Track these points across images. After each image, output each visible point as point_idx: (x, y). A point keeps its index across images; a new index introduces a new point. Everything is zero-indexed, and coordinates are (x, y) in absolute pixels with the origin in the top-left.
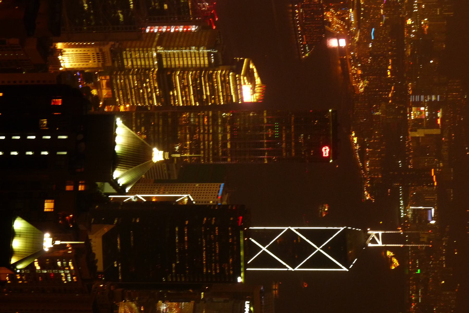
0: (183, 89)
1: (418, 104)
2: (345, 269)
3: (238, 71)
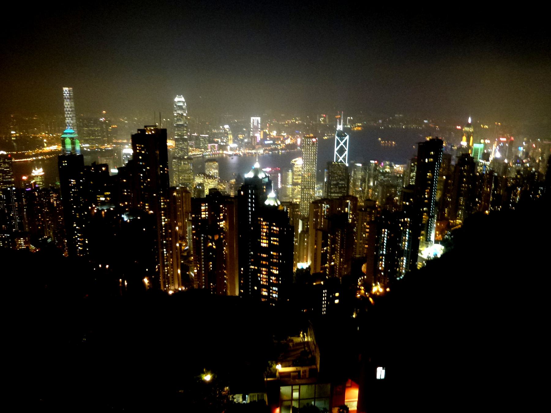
0: (298, 179)
3: (294, 164)
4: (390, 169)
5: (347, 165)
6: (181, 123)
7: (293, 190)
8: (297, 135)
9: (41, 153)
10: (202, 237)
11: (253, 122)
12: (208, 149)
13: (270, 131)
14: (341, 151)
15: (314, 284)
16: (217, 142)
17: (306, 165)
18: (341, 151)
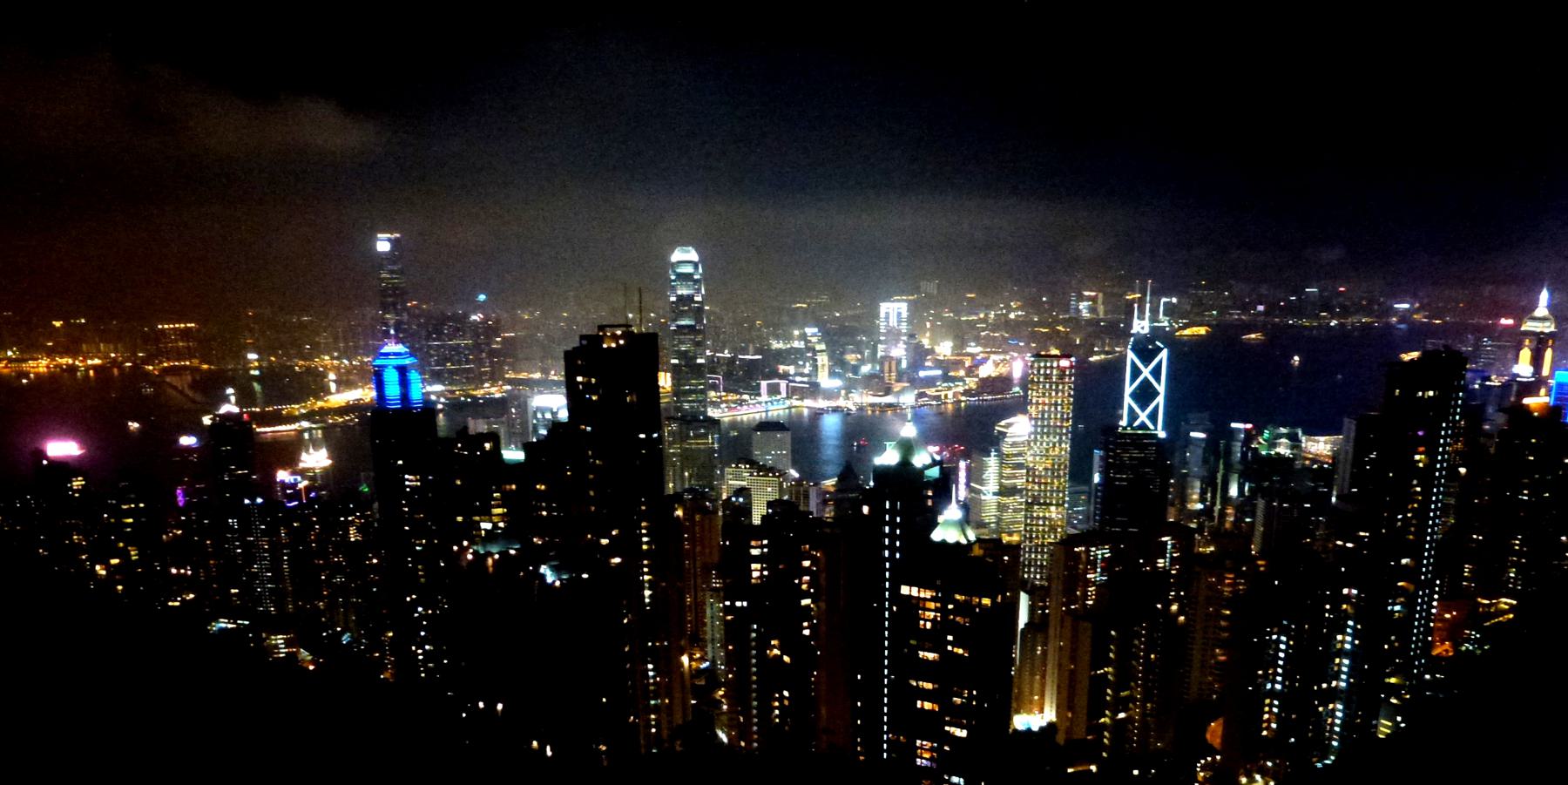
0: (1016, 478)
1: (1078, 311)
2: (1164, 355)
4: (1292, 448)
5: (1162, 434)
6: (683, 323)
7: (1002, 508)
8: (1012, 353)
9: (321, 409)
10: (754, 631)
11: (887, 317)
12: (759, 395)
13: (934, 341)
14: (1145, 395)
15: (1070, 770)
16: (785, 376)
17: (1039, 437)
18: (1145, 395)
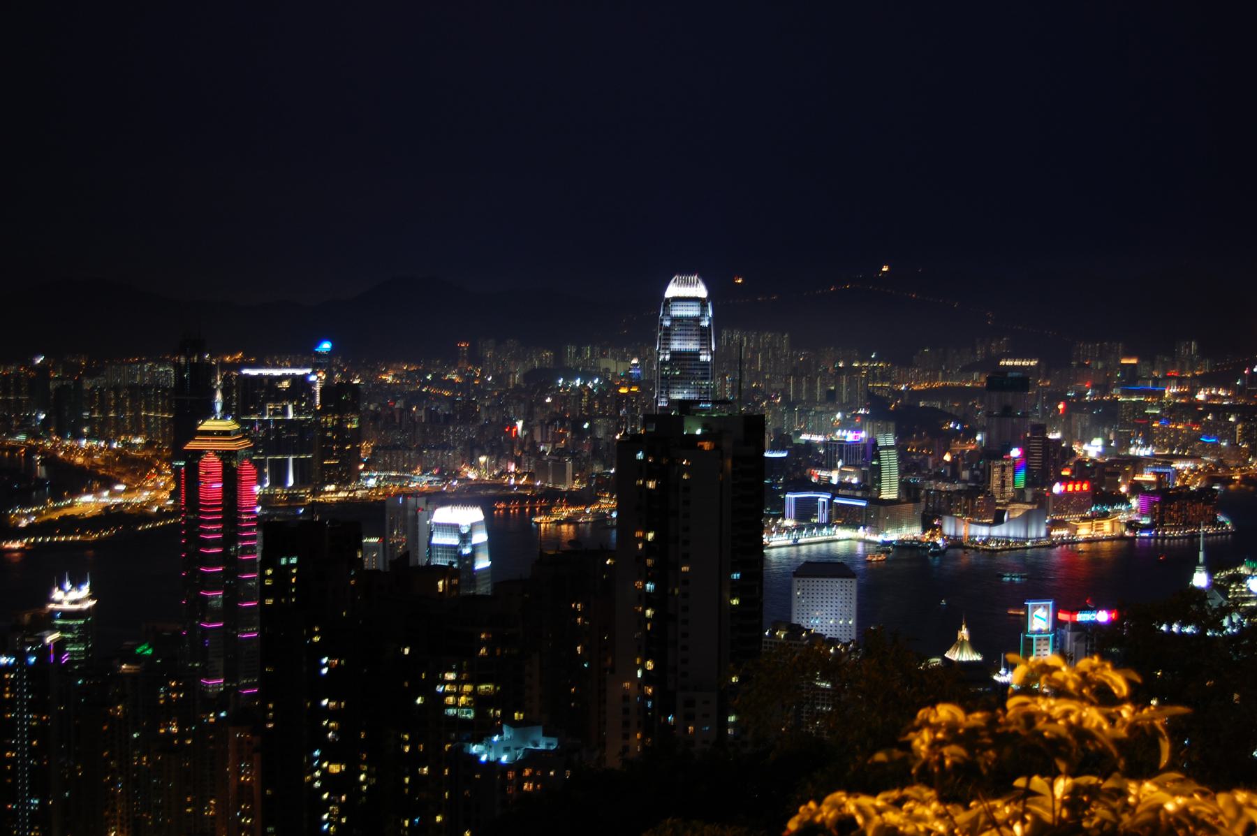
9: (64, 518)
16: (825, 486)
